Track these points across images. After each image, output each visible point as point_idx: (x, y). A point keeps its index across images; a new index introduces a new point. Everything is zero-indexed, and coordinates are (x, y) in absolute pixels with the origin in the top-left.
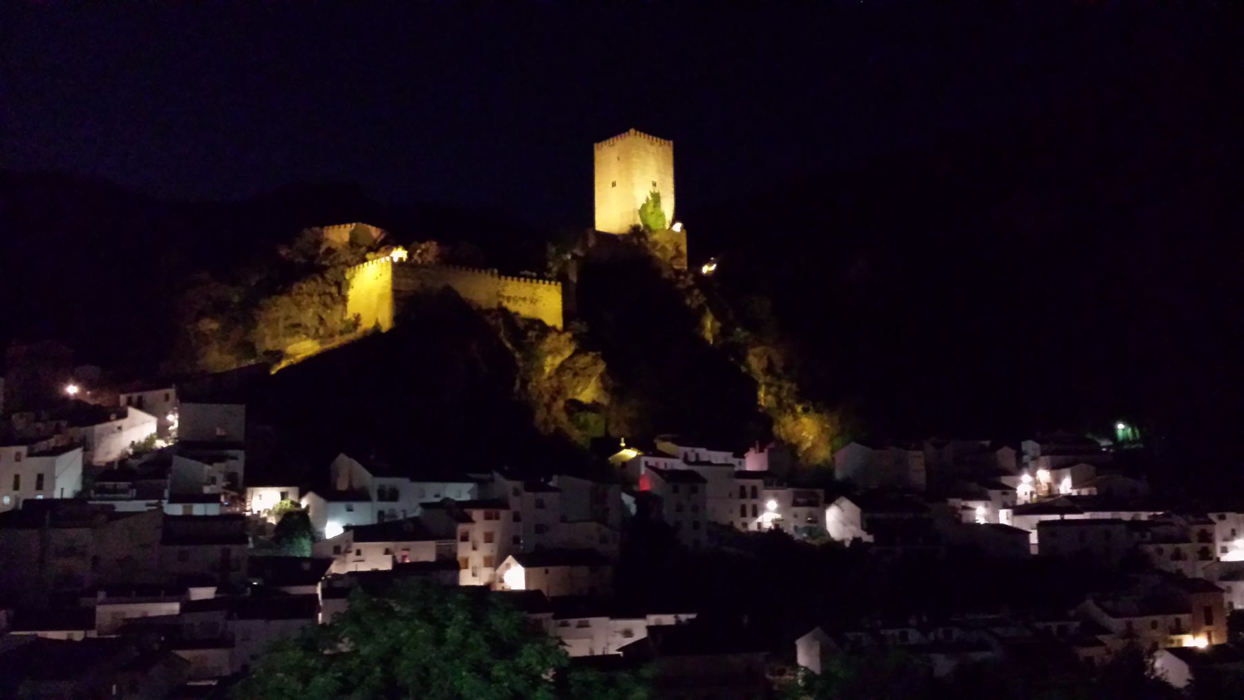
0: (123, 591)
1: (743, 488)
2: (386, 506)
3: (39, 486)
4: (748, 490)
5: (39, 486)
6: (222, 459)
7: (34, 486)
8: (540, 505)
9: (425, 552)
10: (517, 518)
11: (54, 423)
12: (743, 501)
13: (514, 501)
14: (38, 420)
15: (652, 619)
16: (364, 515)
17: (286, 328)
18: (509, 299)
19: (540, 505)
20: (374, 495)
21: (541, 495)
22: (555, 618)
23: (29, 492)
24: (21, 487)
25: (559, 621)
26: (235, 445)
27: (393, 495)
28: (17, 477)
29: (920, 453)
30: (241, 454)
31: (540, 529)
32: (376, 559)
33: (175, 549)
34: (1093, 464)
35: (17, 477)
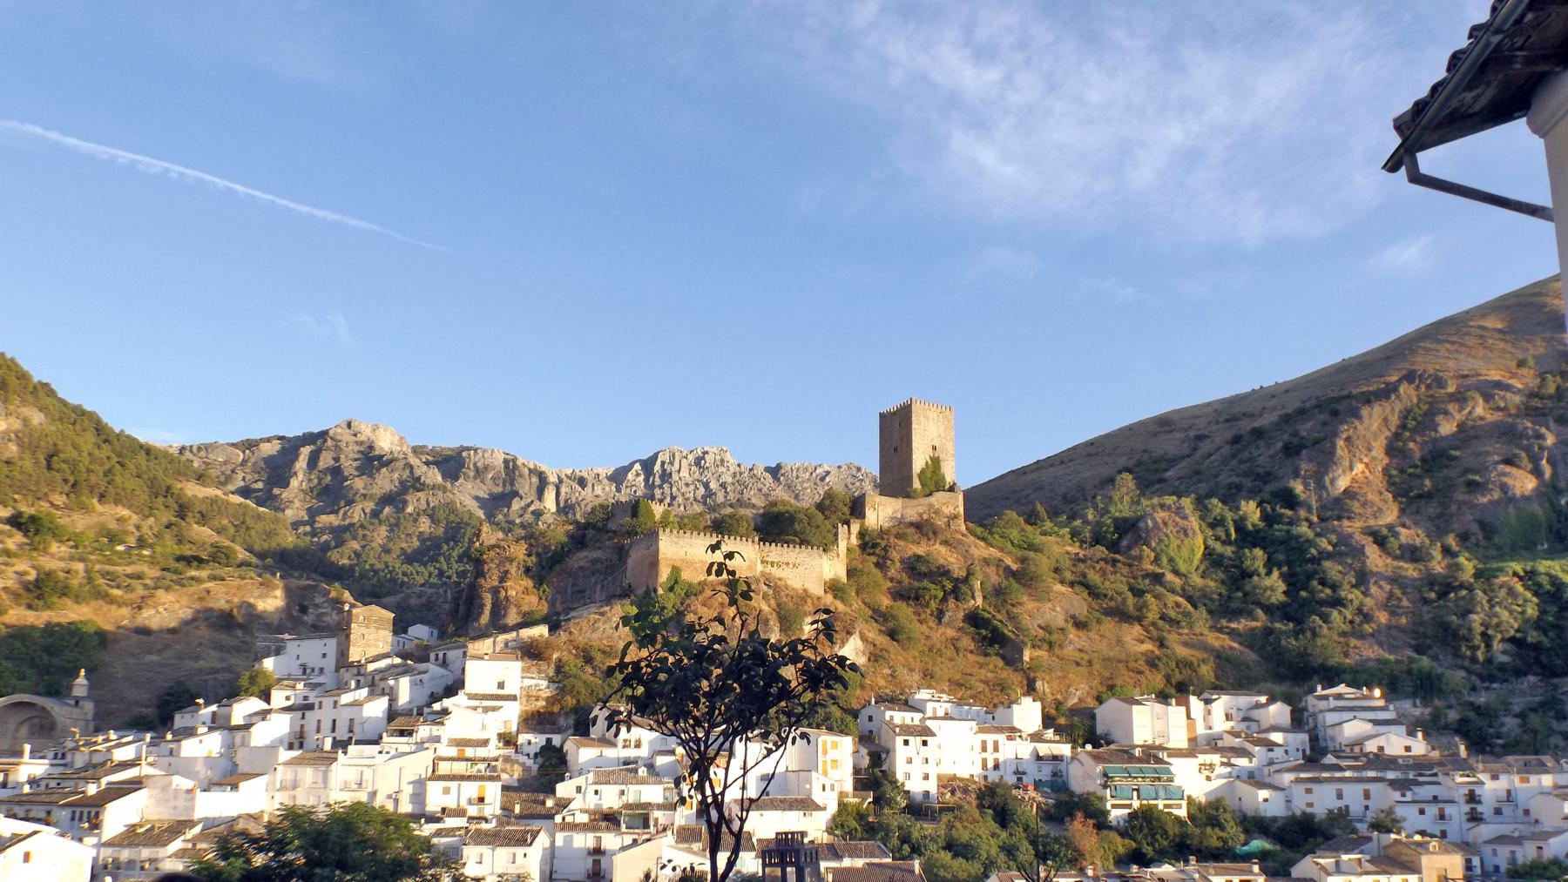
1: (984, 743)
4: (990, 747)
6: (494, 709)
7: (347, 729)
12: (984, 755)
14: (359, 674)
15: (847, 862)
17: (573, 593)
23: (342, 734)
24: (337, 729)
26: (513, 698)
28: (334, 721)
29: (1183, 709)
32: (610, 798)
34: (1370, 721)
35: (334, 721)
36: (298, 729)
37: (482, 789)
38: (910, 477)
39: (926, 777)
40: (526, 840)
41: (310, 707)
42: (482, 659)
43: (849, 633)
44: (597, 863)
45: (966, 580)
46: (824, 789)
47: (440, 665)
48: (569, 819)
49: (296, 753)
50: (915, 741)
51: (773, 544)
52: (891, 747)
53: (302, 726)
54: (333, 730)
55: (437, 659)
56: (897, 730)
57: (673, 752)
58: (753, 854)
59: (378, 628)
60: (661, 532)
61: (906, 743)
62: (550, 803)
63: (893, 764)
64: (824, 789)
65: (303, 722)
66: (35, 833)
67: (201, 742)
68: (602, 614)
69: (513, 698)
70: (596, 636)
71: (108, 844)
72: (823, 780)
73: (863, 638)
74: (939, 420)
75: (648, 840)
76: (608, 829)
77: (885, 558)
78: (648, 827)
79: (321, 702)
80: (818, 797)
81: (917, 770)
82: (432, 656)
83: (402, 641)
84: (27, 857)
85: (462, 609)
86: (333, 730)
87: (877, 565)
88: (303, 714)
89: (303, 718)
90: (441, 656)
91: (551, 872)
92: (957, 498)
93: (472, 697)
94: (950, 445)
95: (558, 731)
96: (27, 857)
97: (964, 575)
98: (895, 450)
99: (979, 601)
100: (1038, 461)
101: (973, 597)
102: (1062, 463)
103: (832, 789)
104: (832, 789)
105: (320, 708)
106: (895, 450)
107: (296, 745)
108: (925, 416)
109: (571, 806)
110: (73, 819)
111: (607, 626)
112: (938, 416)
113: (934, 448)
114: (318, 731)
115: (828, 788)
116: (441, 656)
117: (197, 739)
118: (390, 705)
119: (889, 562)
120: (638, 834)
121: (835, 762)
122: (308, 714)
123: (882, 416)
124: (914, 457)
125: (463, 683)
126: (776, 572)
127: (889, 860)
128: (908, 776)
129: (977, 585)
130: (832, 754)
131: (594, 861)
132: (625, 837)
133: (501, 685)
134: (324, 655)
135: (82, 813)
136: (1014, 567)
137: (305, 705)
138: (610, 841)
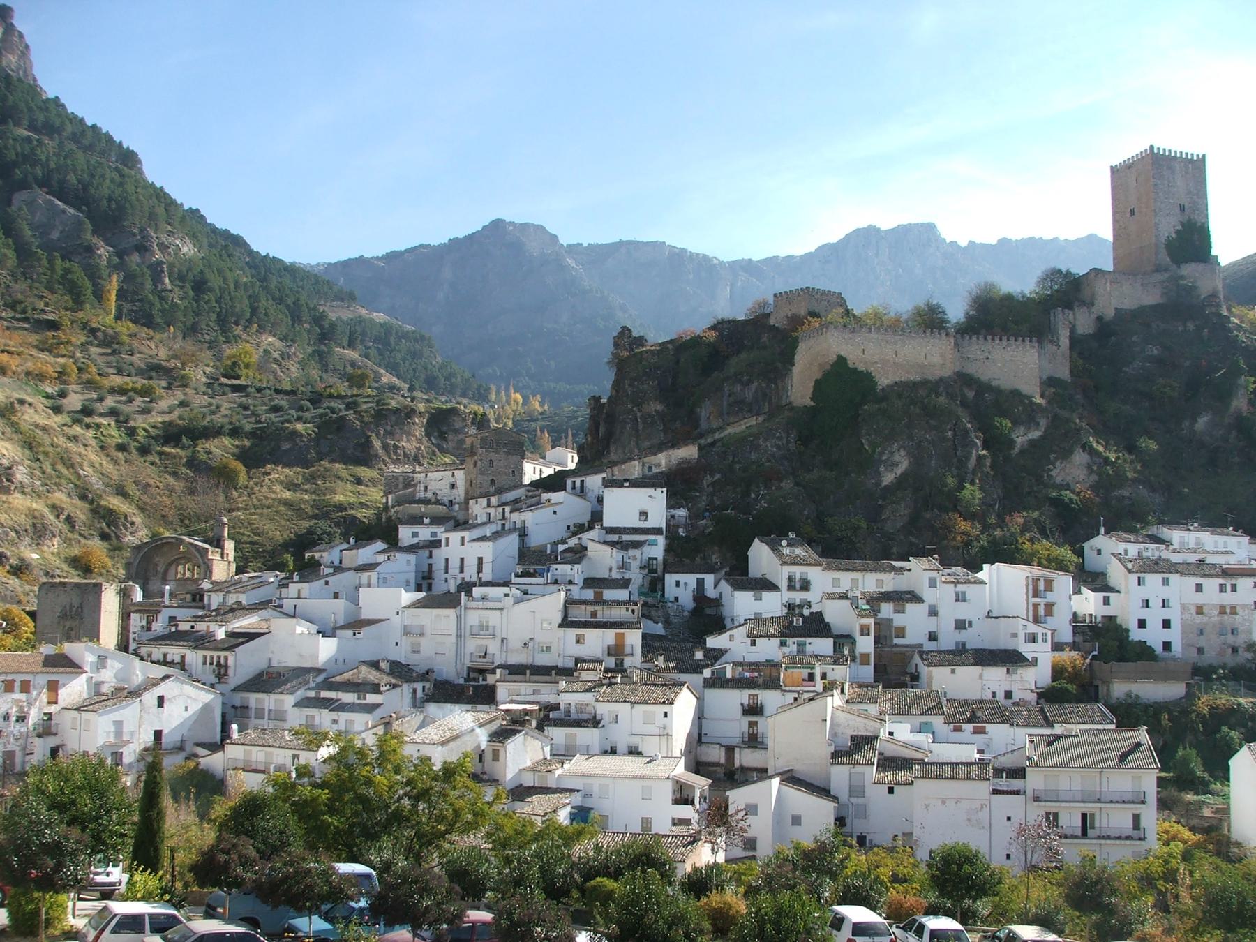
0: (516, 671)
2: (797, 597)
3: (480, 570)
5: (480, 570)
6: (637, 545)
7: (475, 569)
8: (960, 598)
9: (823, 646)
10: (933, 612)
11: (500, 509)
13: (929, 595)
16: (772, 604)
17: (730, 405)
19: (960, 598)
20: (784, 584)
21: (960, 588)
25: (951, 726)
27: (806, 586)
28: (462, 559)
30: (661, 540)
31: (960, 625)
32: (768, 649)
33: (572, 633)
35: (462, 559)
36: (426, 569)
37: (620, 637)
39: (1166, 624)
41: (435, 544)
42: (621, 486)
47: (575, 495)
49: (422, 595)
50: (1153, 580)
51: (974, 338)
53: (430, 565)
54: (462, 571)
55: (574, 488)
59: (508, 453)
62: (699, 655)
65: (430, 561)
66: (167, 677)
67: (327, 583)
69: (657, 531)
71: (238, 689)
72: (1032, 628)
75: (811, 700)
79: (447, 539)
80: (1026, 649)
81: (1155, 617)
82: (569, 482)
83: (538, 468)
84: (161, 701)
85: (602, 430)
86: (462, 571)
88: (431, 552)
89: (430, 556)
90: (578, 484)
91: (700, 735)
93: (611, 530)
95: (710, 570)
96: (161, 701)
98: (1133, 213)
103: (1045, 641)
105: (447, 545)
107: (425, 586)
110: (205, 663)
111: (768, 444)
113: (1182, 208)
114: (447, 572)
115: (1040, 638)
116: (578, 484)
117: (323, 581)
118: (522, 542)
120: (798, 692)
122: (435, 551)
123: (1114, 171)
125: (601, 520)
127: (1113, 727)
128: (1142, 624)
133: (644, 514)
134: (453, 486)
135: (212, 658)
137: (431, 542)
138: (769, 698)
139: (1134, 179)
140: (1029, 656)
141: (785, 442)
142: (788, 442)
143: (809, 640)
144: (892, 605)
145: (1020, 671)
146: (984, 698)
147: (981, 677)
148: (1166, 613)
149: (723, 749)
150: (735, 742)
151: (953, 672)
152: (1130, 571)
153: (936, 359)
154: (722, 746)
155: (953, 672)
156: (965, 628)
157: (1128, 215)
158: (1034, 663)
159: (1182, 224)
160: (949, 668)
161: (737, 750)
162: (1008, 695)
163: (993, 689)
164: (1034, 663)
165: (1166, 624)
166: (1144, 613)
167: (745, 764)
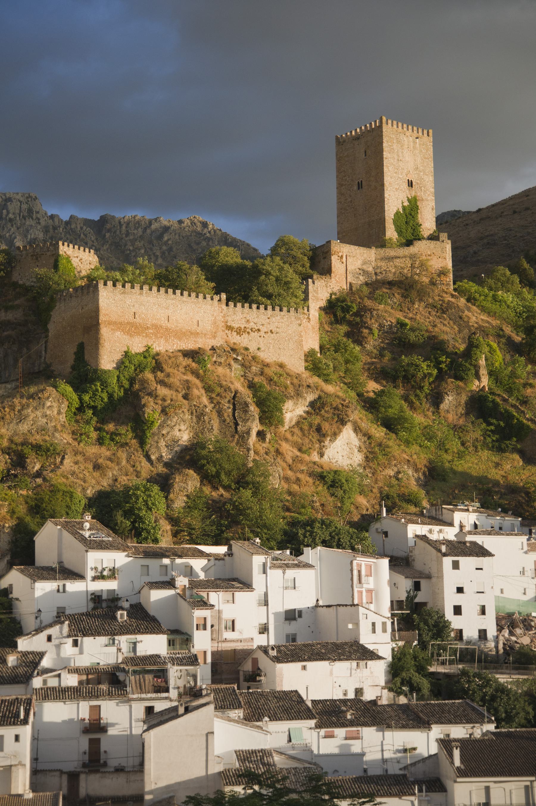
18: (239, 332)
21: (291, 573)
22: (319, 726)
25: (323, 732)
38: (382, 221)
40: (18, 715)
43: (343, 422)
44: (95, 744)
45: (468, 354)
46: (374, 631)
48: (53, 683)
51: (239, 305)
52: (434, 572)
56: (444, 549)
57: (170, 584)
58: (312, 723)
60: (101, 285)
61: (456, 565)
62: (12, 660)
63: (438, 593)
64: (374, 631)
68: (31, 397)
70: (24, 427)
73: (357, 429)
74: (414, 148)
76: (110, 695)
77: (364, 325)
78: (167, 690)
87: (348, 335)
92: (443, 250)
94: (429, 181)
97: (462, 347)
98: (360, 186)
99: (485, 381)
100: (455, 211)
101: (478, 378)
102: (515, 212)
104: (384, 630)
106: (360, 186)
108: (399, 142)
109: (45, 663)
111: (39, 413)
112: (415, 142)
113: (410, 184)
115: (379, 627)
119: (366, 331)
121: (369, 591)
124: (386, 195)
126: (243, 341)
128: (458, 610)
129: (482, 362)
130: (370, 583)
131: (91, 741)
132: (134, 705)
136: (518, 339)
139: (363, 151)
140: (371, 647)
141: (55, 412)
142: (59, 413)
143: (139, 637)
144: (221, 594)
145: (370, 663)
146: (335, 698)
147: (331, 673)
148: (482, 600)
149: (65, 778)
150: (71, 767)
151: (304, 668)
152: (445, 555)
153: (207, 326)
154: (61, 772)
155: (304, 668)
156: (295, 619)
157: (356, 188)
158: (371, 655)
159: (409, 200)
160: (300, 664)
161: (82, 777)
162: (359, 692)
163: (344, 687)
164: (371, 655)
165: (483, 611)
166: (459, 599)
167: (91, 793)
